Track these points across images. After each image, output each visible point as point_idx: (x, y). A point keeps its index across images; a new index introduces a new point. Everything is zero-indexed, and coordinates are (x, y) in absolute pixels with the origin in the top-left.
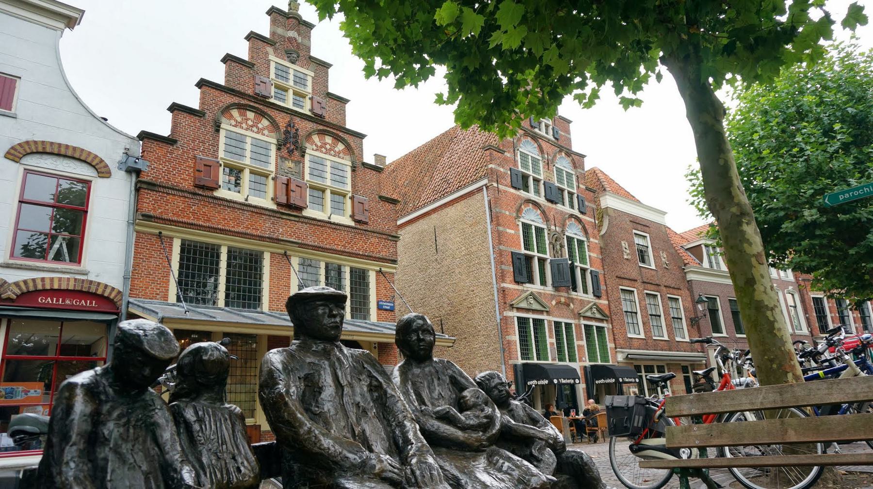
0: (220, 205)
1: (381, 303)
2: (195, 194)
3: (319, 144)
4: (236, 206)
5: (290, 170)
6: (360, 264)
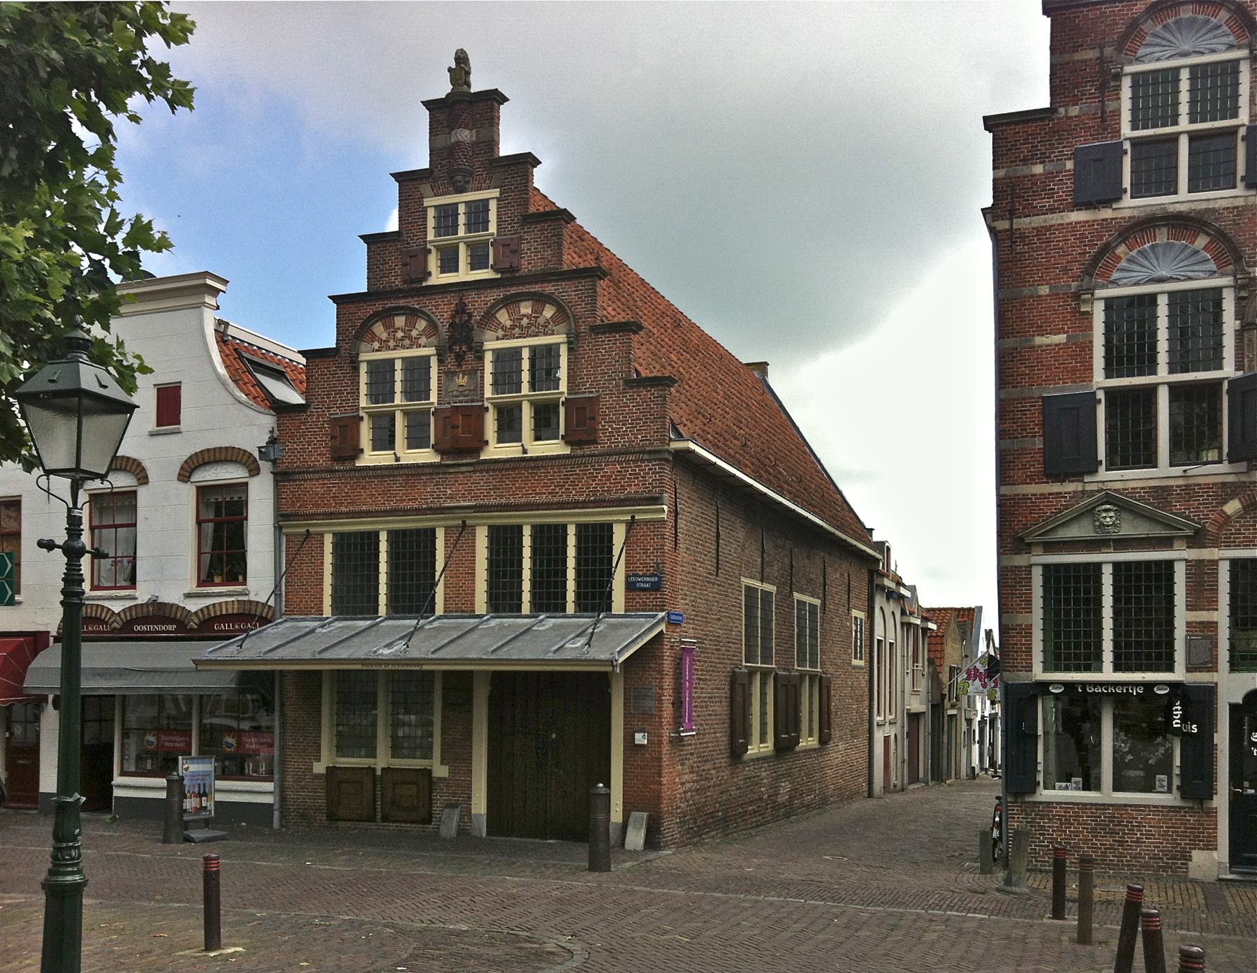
0: (364, 478)
1: (633, 579)
2: (332, 471)
3: (508, 323)
4: (384, 472)
5: (461, 389)
6: (595, 517)
